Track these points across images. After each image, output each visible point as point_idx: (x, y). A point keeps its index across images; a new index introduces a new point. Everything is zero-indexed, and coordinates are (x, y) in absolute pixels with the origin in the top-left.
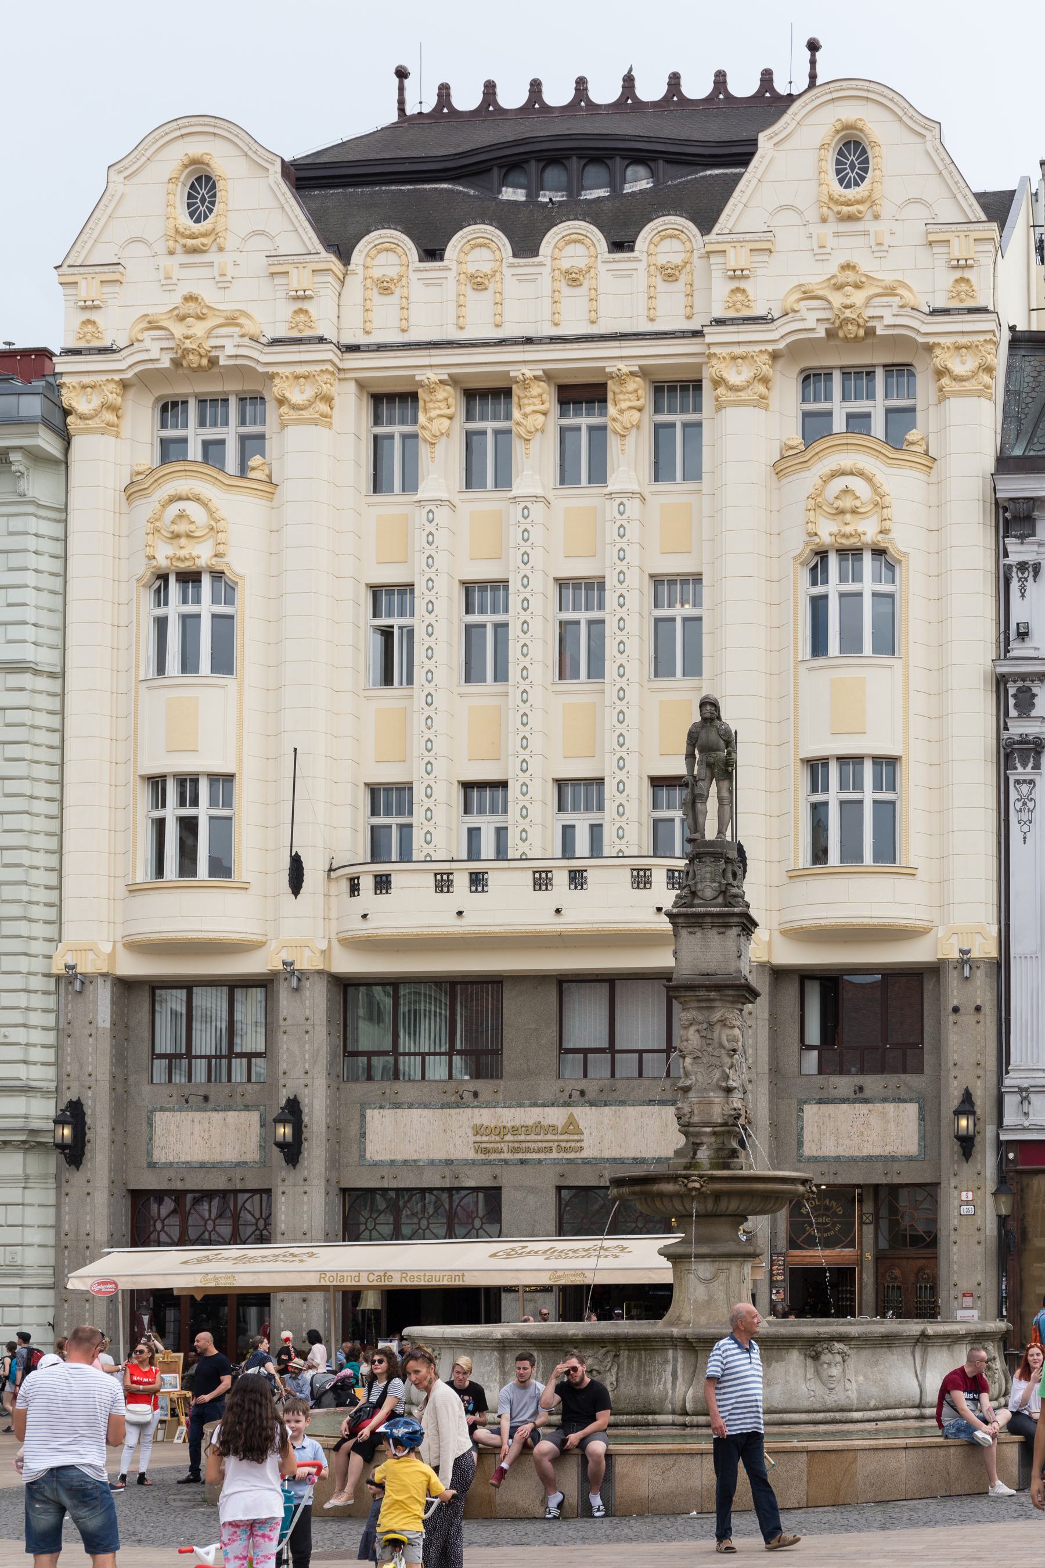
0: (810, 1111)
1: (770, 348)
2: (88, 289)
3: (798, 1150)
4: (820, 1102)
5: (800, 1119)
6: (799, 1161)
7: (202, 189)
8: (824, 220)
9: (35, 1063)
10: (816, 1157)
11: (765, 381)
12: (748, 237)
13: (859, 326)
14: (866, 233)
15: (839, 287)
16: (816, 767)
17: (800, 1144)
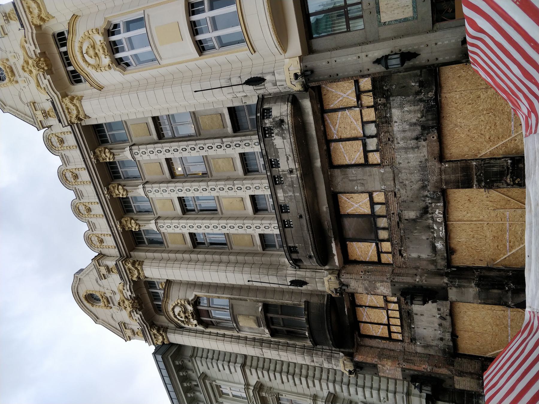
0: (385, 17)
1: (60, 97)
2: (129, 333)
3: (410, 20)
4: (378, 12)
5: (390, 23)
6: (417, 18)
7: (91, 298)
8: (17, 82)
9: (396, 388)
10: (413, 7)
11: (72, 99)
12: (32, 113)
13: (40, 60)
14: (15, 64)
15: (31, 72)
16: (201, 48)
17: (406, 20)
